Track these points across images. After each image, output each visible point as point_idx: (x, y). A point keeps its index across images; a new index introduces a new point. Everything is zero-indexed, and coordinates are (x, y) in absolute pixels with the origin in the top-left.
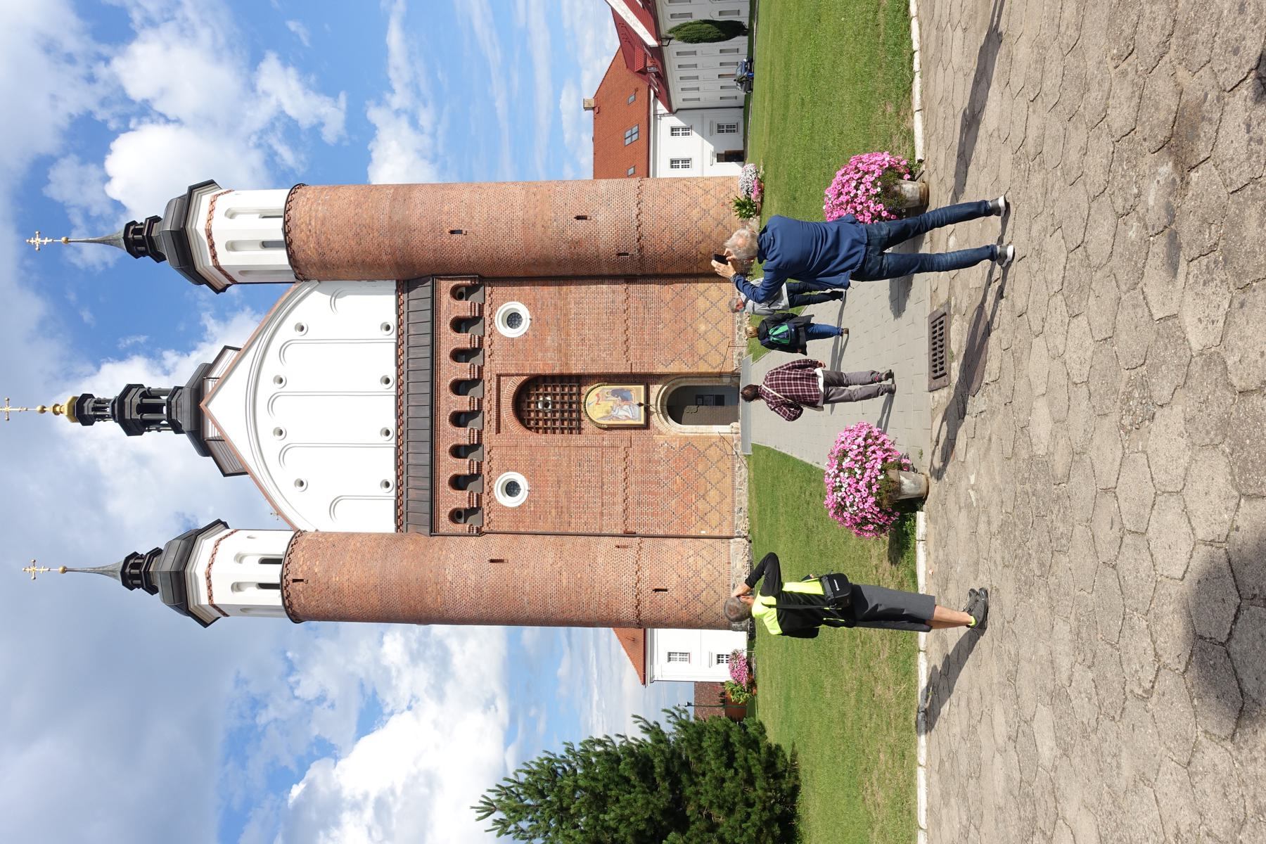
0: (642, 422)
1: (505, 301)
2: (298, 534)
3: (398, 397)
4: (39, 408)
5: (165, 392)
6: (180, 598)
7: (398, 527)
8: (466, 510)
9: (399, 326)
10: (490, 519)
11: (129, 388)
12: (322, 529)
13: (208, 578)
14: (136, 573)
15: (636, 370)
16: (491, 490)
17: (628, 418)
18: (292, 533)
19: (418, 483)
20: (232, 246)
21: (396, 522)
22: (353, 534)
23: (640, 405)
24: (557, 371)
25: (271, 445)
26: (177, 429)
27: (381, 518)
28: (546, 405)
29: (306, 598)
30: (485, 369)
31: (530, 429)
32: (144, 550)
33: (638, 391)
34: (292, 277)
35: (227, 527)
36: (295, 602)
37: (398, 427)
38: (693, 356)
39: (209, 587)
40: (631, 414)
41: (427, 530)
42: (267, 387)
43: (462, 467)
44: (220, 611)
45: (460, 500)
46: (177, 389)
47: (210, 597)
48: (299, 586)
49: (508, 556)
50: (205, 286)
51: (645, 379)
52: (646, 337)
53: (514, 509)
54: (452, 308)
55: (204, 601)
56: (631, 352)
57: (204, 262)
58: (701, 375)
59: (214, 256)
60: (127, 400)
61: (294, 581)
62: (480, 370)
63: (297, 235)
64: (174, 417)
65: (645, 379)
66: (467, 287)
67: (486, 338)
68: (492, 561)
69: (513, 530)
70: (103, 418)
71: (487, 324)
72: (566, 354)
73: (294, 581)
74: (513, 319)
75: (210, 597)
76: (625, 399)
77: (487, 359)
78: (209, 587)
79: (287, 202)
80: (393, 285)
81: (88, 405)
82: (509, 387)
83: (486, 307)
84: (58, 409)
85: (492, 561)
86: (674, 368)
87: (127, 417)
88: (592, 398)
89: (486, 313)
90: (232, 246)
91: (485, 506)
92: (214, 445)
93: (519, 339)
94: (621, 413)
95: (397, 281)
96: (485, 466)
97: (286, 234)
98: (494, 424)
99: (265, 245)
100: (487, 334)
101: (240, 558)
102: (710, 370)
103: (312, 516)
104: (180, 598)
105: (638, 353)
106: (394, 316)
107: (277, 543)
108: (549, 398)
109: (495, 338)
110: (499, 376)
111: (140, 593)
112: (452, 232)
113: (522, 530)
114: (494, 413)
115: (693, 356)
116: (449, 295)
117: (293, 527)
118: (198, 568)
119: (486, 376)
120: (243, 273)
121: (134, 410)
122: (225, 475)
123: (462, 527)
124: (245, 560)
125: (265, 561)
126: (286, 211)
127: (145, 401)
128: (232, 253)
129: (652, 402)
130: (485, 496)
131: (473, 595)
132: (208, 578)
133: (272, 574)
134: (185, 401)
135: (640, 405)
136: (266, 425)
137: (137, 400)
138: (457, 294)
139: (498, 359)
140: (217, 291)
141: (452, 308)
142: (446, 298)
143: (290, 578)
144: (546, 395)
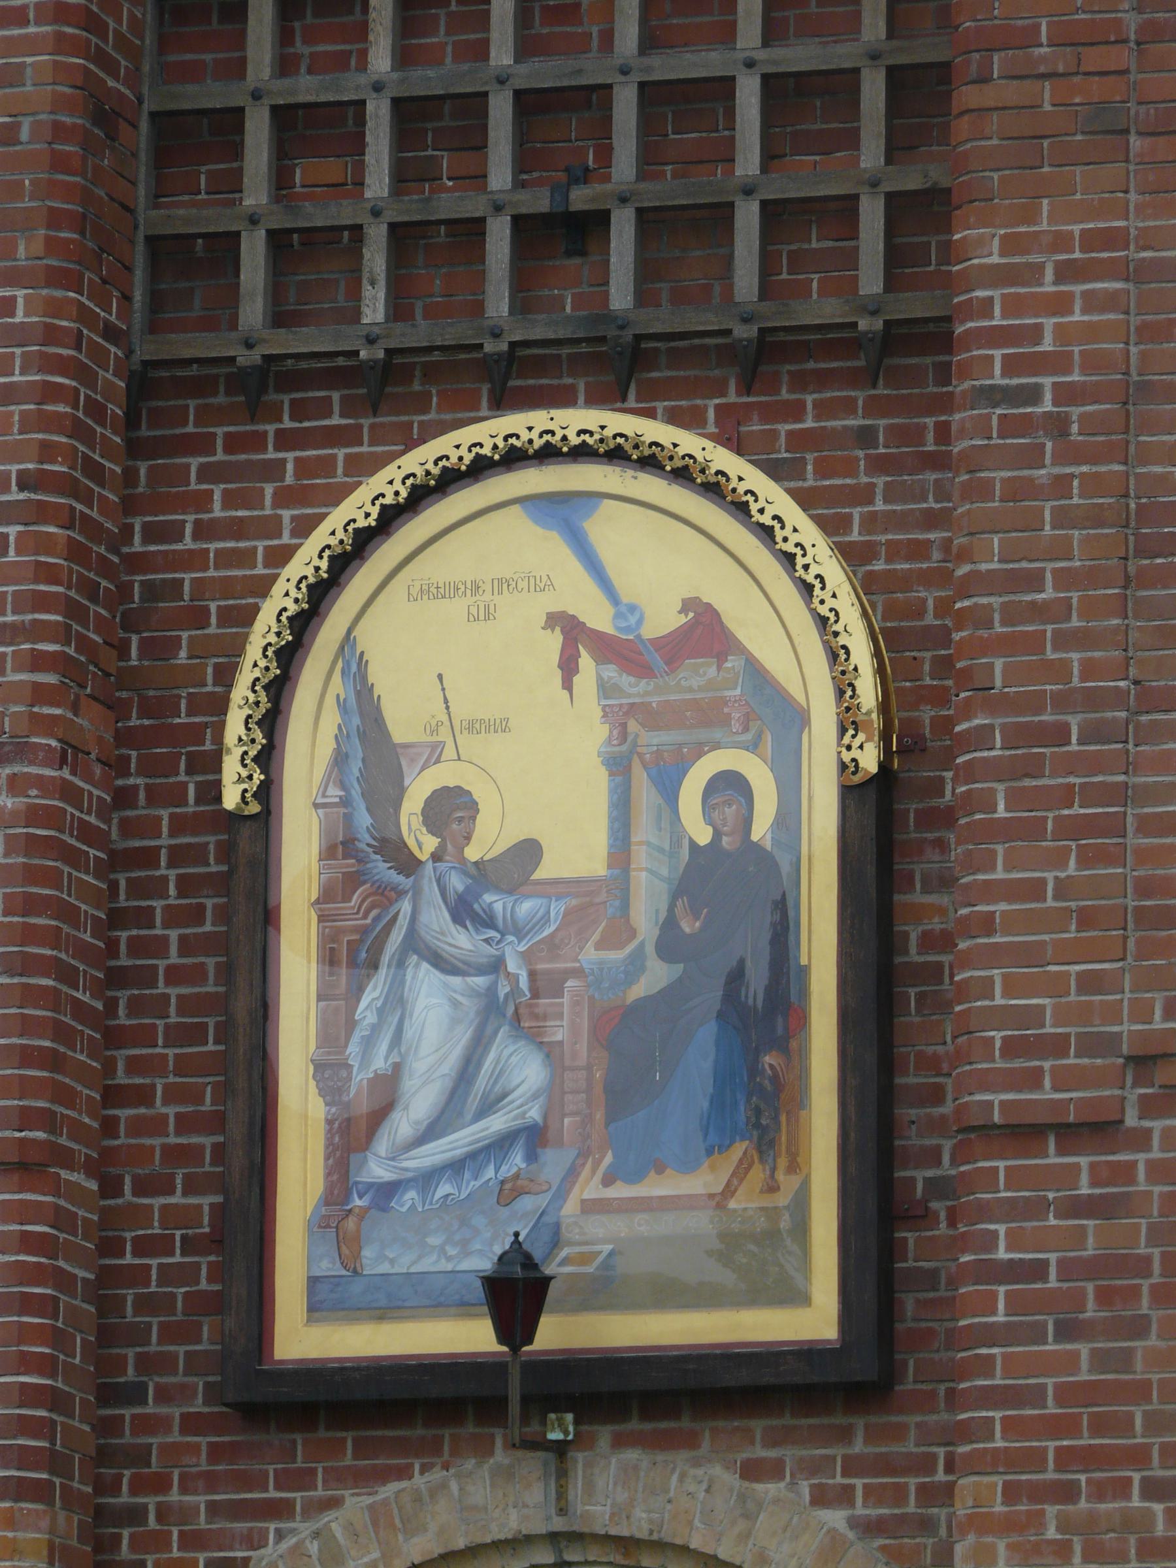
15: (1011, 1227)
94: (431, 1017)
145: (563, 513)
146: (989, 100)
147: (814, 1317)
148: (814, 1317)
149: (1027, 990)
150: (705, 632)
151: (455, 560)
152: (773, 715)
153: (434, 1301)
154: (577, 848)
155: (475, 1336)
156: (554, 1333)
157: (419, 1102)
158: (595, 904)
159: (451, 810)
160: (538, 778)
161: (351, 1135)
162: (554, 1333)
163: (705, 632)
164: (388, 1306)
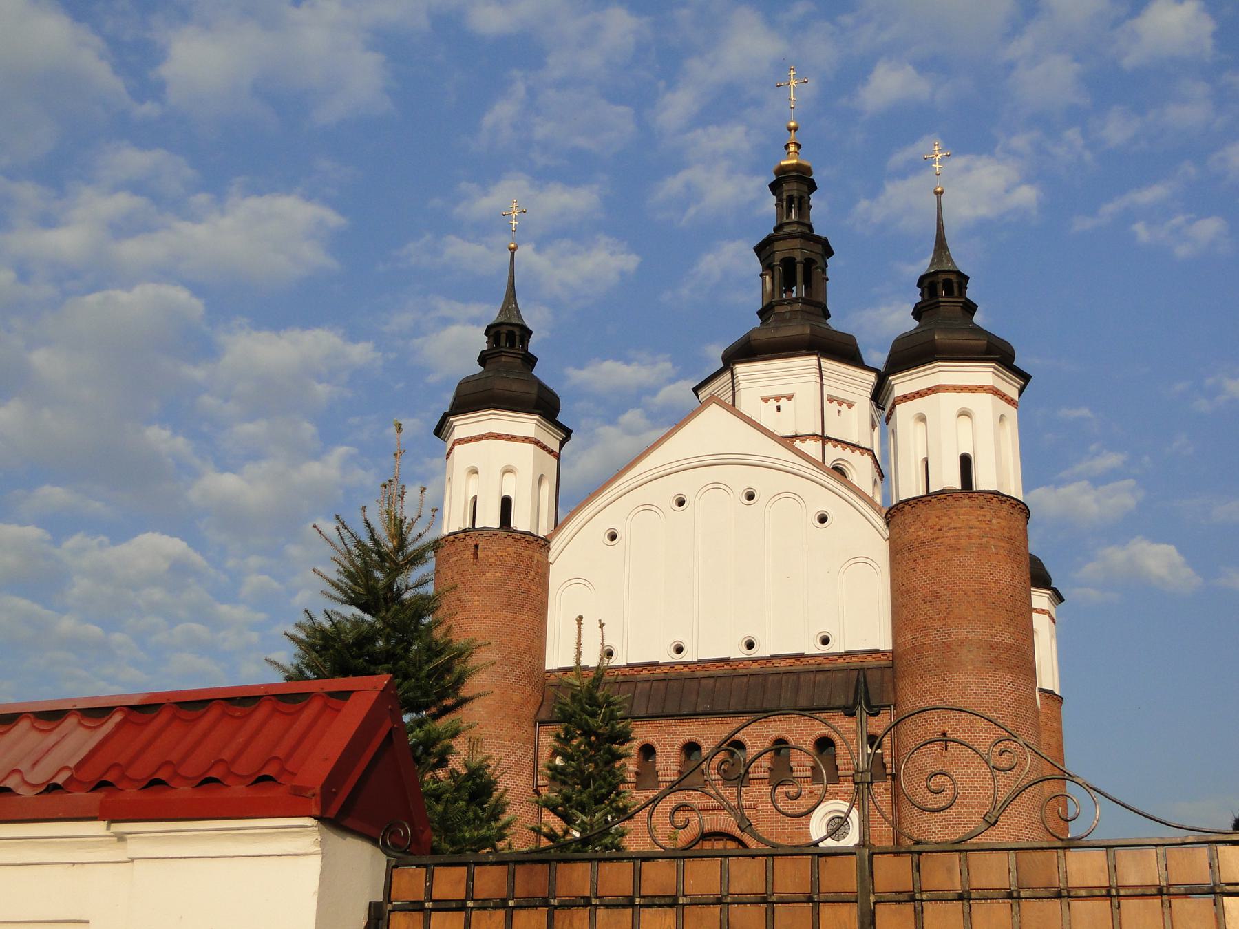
2: (544, 544)
6: (470, 399)
7: (551, 672)
9: (826, 656)
18: (543, 533)
36: (453, 549)
41: (544, 716)
42: (743, 479)
47: (462, 441)
48: (469, 554)
59: (906, 398)
60: (797, 242)
63: (932, 515)
73: (477, 546)
75: (462, 441)
80: (885, 644)
87: (779, 246)
127: (800, 268)
133: (489, 518)
143: (481, 542)
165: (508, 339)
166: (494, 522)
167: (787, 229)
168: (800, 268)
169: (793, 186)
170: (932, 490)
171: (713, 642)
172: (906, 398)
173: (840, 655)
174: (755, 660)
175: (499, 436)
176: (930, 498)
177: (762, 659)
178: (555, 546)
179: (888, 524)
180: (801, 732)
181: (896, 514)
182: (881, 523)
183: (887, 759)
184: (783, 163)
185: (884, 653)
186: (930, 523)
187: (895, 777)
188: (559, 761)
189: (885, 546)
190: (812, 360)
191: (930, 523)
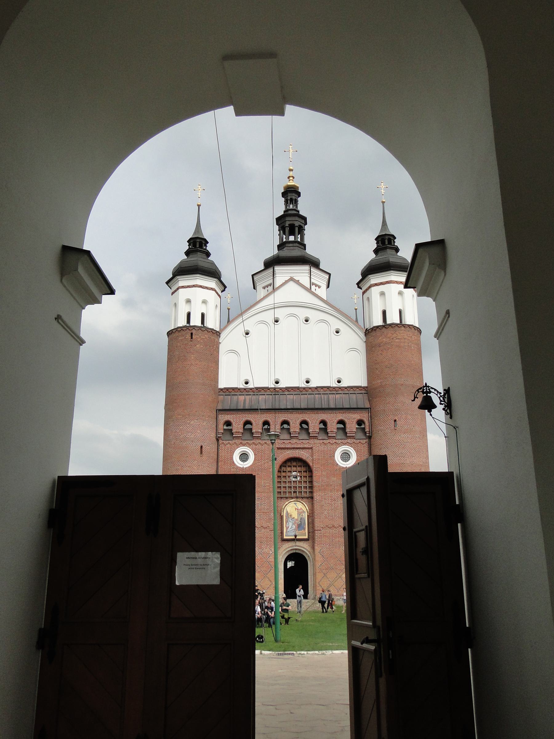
0: (285, 537)
1: (357, 451)
2: (218, 334)
3: (298, 388)
4: (291, 168)
5: (302, 238)
7: (221, 390)
8: (231, 430)
9: (340, 388)
10: (226, 444)
11: (305, 219)
12: (221, 346)
13: (194, 286)
14: (197, 245)
15: (317, 534)
16: (244, 445)
17: (287, 528)
18: (218, 330)
19: (247, 402)
20: (382, 294)
21: (225, 388)
22: (218, 365)
23: (296, 536)
24: (315, 484)
25: (269, 316)
26: (280, 247)
27: (228, 378)
28: (296, 477)
29: (182, 340)
30: (316, 441)
31: (281, 467)
32: (209, 248)
33: (305, 535)
34: (368, 326)
35: (222, 292)
36: (180, 334)
37: (281, 389)
38: (326, 569)
39: (189, 287)
40: (290, 530)
42: (303, 313)
43: (257, 428)
44: (175, 291)
45: (237, 427)
46: (304, 246)
47: (183, 287)
48: (188, 336)
49: (205, 457)
50: (360, 277)
51: (311, 539)
52: (337, 539)
53: (232, 458)
54: (351, 419)
55: (181, 284)
56: (328, 530)
57: (374, 279)
58: (314, 574)
59: (376, 285)
60: (297, 218)
61: (192, 334)
62: (315, 437)
63: (389, 332)
64: (287, 245)
65: (311, 539)
66: (364, 429)
67: (334, 441)
68: (201, 447)
69: (220, 459)
70: (286, 202)
71: (342, 441)
72: (325, 490)
73: (192, 334)
74: (346, 456)
75: (183, 287)
76: (300, 526)
77: (322, 441)
78: (189, 287)
79: (409, 325)
80: (364, 384)
81: (294, 196)
82: (304, 455)
83: (353, 440)
84: (291, 178)
85: (201, 447)
86: (319, 557)
87: (288, 219)
88: (300, 505)
89: (349, 441)
90: (382, 294)
91: (234, 441)
92: (271, 270)
93: (334, 460)
94: (290, 524)
95: (367, 387)
96: (257, 441)
97: (390, 325)
98: (283, 446)
99: (384, 313)
100: (337, 441)
101: (204, 302)
102: (317, 581)
103: (229, 341)
104: (182, 271)
105: (327, 534)
106: (346, 385)
107: (212, 323)
108: (299, 478)
109: (334, 446)
110: (311, 448)
111: (186, 247)
112: (395, 421)
113: (220, 464)
114: (289, 446)
115: (326, 569)
116: (359, 418)
117: (222, 330)
118: (200, 280)
119: (312, 441)
120: (368, 299)
121: (291, 222)
122: (253, 276)
123: (222, 427)
124: (204, 305)
125: (203, 315)
126: (405, 326)
127: (297, 229)
128: (379, 295)
129: (298, 543)
130: (240, 441)
131: (182, 437)
132: (194, 286)
134: (296, 252)
135: (296, 536)
136: (280, 313)
137: (297, 224)
138: (360, 423)
139: (322, 448)
140: (358, 284)
141: (351, 419)
142: (357, 416)
143: (194, 331)
144: (301, 477)
145: (295, 504)
146: (315, 489)
147: (307, 537)
148: (307, 537)
149: (318, 524)
150: (301, 509)
151: (291, 505)
152: (304, 512)
153: (291, 536)
154: (296, 518)
155: (294, 537)
156: (297, 537)
157: (290, 528)
158: (297, 520)
159: (291, 516)
160: (295, 515)
161: (287, 528)
162: (297, 537)
163: (301, 509)
164: (289, 536)
165: (197, 245)
166: (199, 324)
167: (290, 212)
168: (297, 229)
169: (291, 194)
170: (389, 322)
171: (290, 380)
172: (376, 285)
173: (346, 388)
174: (310, 388)
175: (201, 287)
176: (386, 326)
177: (313, 388)
178: (223, 335)
179: (366, 335)
180: (332, 419)
181: (367, 332)
182: (362, 335)
183: (367, 430)
184: (289, 184)
185: (364, 388)
186: (388, 336)
187: (370, 438)
188: (225, 427)
189: (364, 345)
190: (307, 267)
191: (388, 336)
